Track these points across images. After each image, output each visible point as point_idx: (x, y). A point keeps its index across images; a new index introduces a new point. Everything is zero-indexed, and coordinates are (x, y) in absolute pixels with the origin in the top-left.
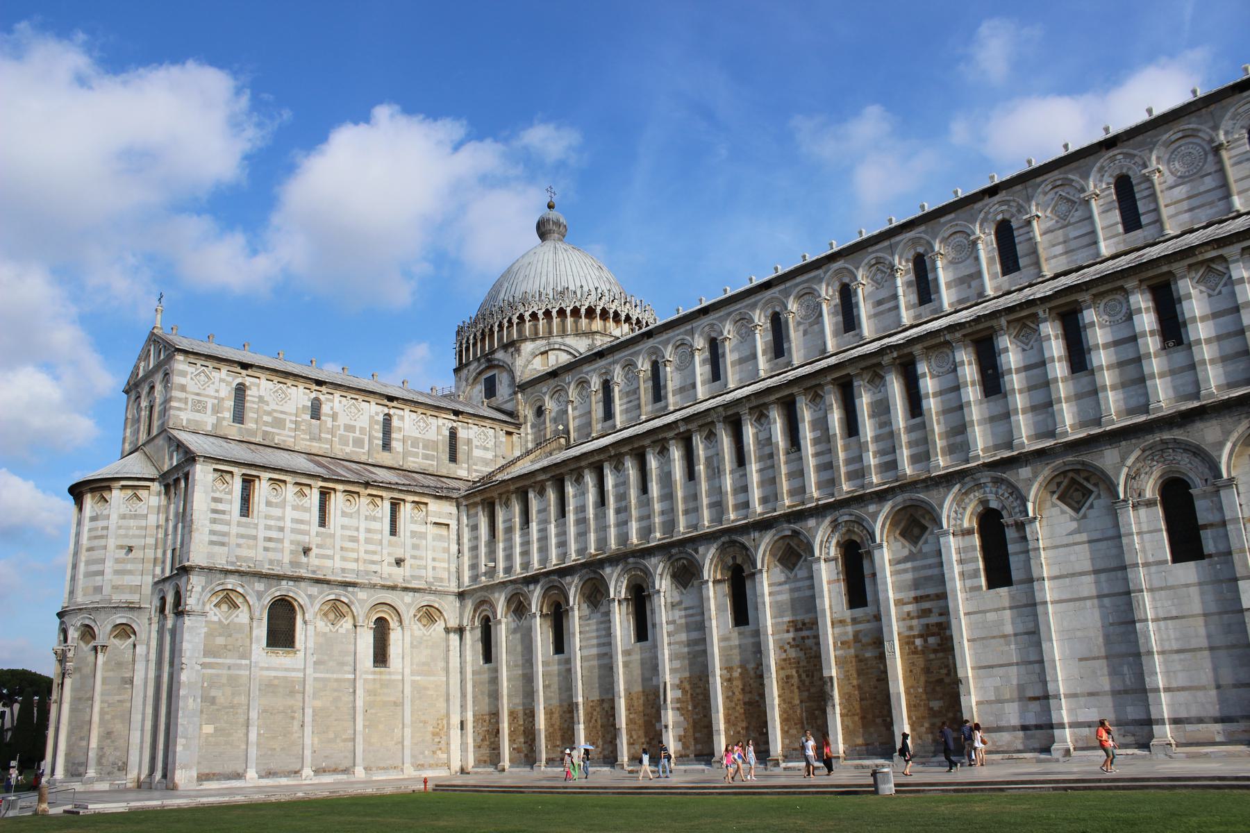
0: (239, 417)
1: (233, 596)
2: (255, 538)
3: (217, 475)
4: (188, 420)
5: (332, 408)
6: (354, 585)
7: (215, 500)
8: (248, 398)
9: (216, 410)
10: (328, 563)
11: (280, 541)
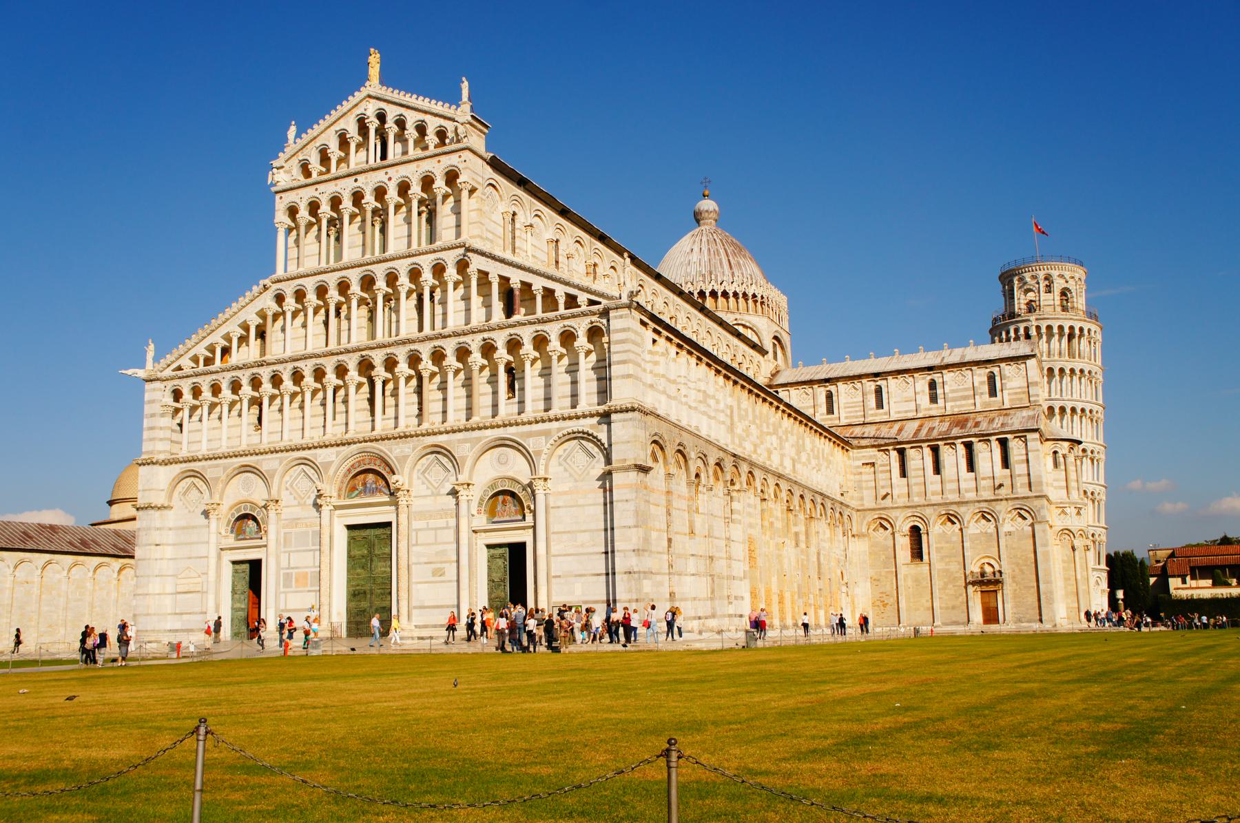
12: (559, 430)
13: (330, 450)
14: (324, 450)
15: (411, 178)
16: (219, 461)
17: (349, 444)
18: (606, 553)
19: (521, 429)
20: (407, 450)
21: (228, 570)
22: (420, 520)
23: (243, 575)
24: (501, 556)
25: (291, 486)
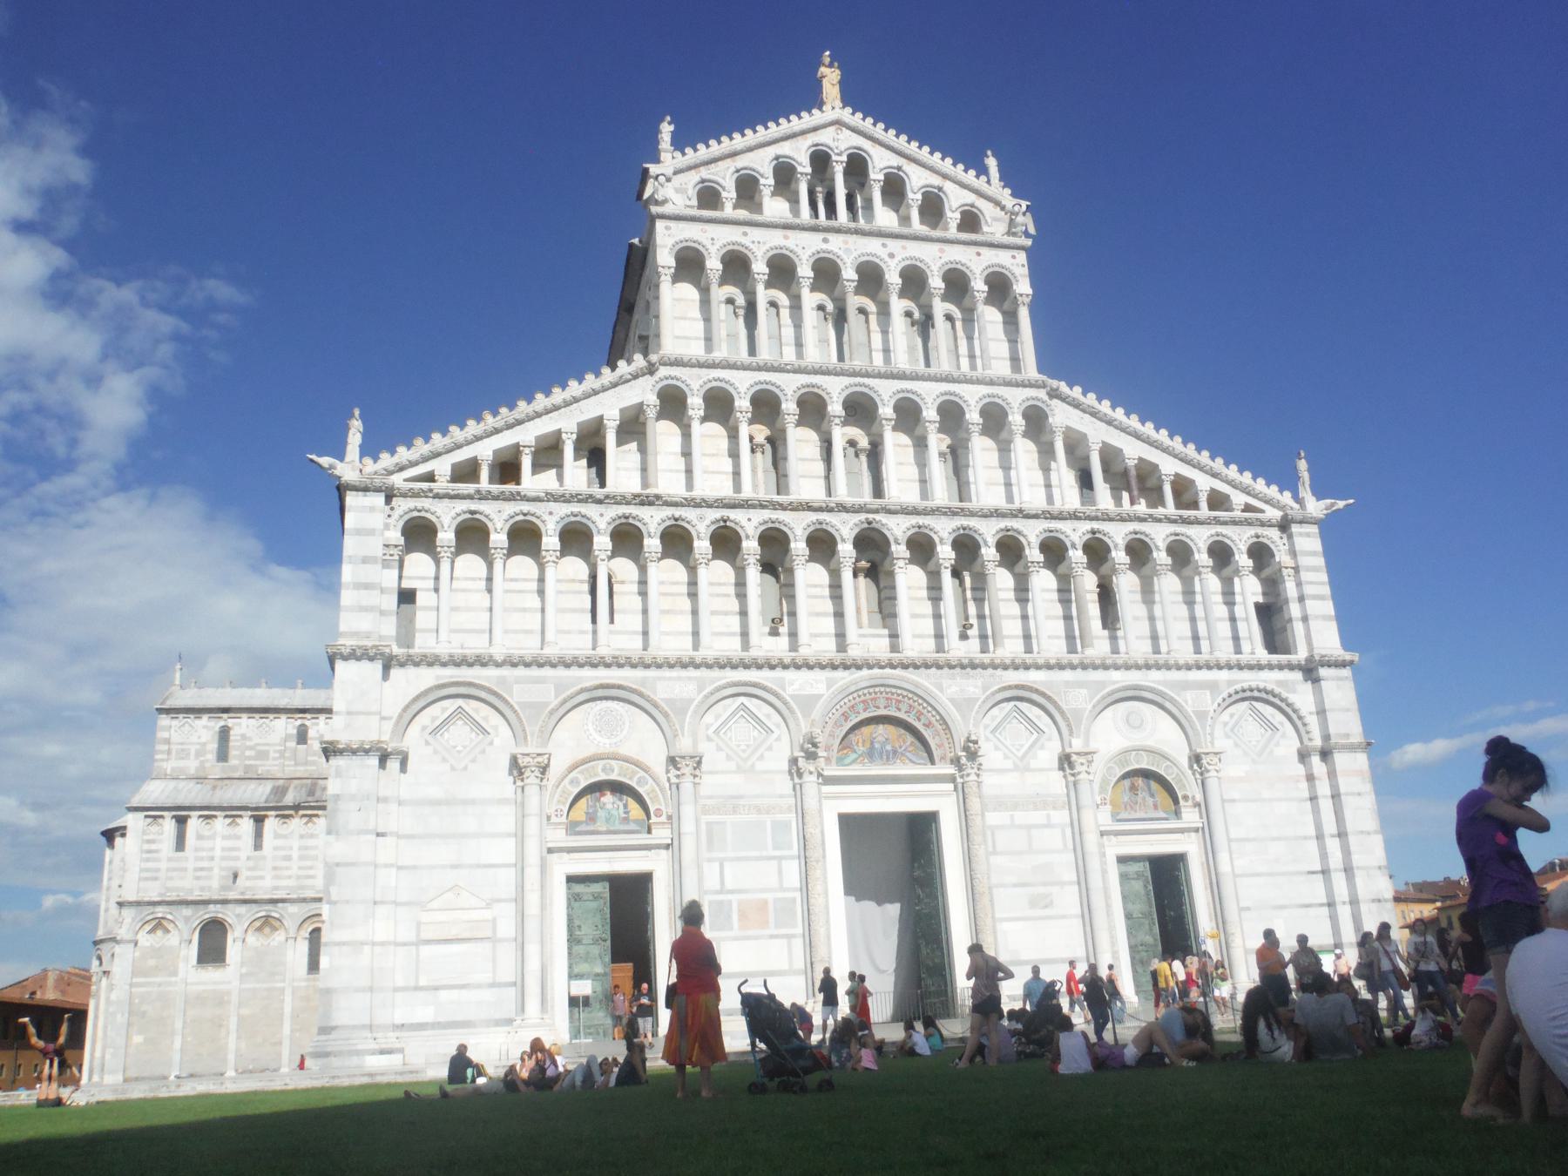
0: (223, 755)
1: (165, 923)
2: (185, 870)
3: (149, 820)
4: (173, 769)
5: (318, 731)
6: (283, 901)
7: (149, 842)
8: (231, 738)
9: (198, 754)
10: (260, 883)
11: (210, 869)
12: (1230, 683)
13: (817, 674)
14: (805, 674)
15: (930, 263)
16: (547, 672)
17: (859, 668)
18: (1325, 872)
19: (1175, 675)
20: (972, 689)
21: (559, 893)
22: (995, 810)
23: (594, 905)
24: (1139, 875)
25: (716, 732)
